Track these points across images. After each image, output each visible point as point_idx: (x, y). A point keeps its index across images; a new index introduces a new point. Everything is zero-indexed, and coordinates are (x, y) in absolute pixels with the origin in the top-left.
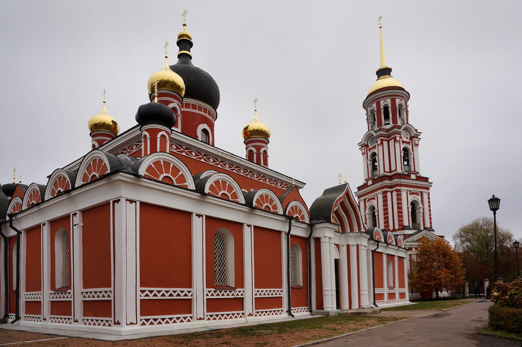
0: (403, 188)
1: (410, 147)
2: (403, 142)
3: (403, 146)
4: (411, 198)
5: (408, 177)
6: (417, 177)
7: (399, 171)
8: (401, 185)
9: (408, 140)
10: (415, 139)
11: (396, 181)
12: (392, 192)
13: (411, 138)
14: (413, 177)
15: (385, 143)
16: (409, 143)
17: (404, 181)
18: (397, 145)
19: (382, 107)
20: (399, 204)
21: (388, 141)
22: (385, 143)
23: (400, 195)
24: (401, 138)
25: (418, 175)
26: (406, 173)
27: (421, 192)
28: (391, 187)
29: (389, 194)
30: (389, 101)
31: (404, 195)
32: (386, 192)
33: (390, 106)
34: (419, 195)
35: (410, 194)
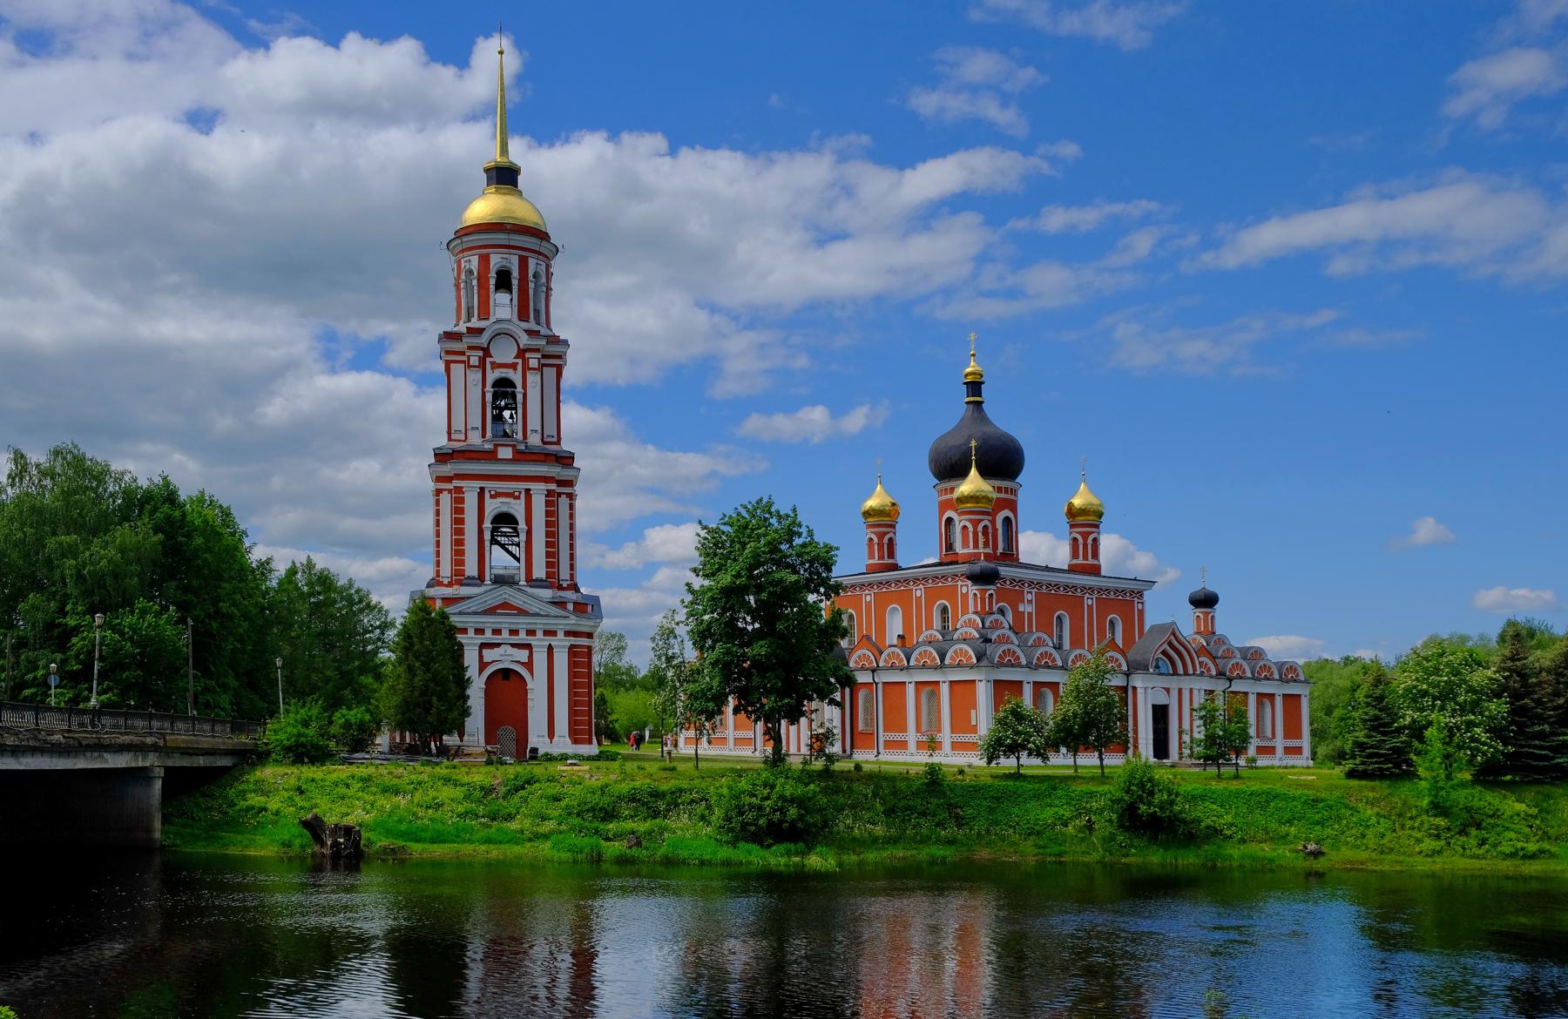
1: (516, 377)
2: (495, 366)
3: (492, 376)
4: (493, 507)
5: (491, 456)
6: (516, 452)
7: (475, 439)
9: (510, 359)
10: (528, 355)
12: (450, 491)
13: (521, 353)
14: (505, 453)
15: (458, 370)
16: (513, 366)
20: (458, 521)
22: (458, 370)
23: (462, 500)
24: (487, 352)
26: (488, 446)
27: (528, 491)
34: (518, 498)
35: (492, 497)
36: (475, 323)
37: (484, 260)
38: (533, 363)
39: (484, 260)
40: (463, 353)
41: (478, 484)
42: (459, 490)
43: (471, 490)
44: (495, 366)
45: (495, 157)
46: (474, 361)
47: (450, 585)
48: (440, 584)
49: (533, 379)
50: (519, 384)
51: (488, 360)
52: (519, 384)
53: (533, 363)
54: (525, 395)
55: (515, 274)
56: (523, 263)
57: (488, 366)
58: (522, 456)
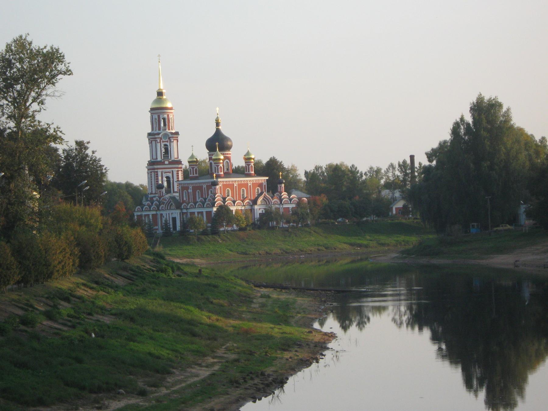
0: (159, 170)
1: (168, 144)
2: (163, 142)
5: (163, 163)
7: (159, 159)
8: (158, 169)
11: (156, 167)
13: (169, 138)
14: (166, 162)
15: (154, 143)
16: (167, 141)
17: (159, 166)
18: (159, 145)
22: (154, 143)
23: (157, 174)
28: (154, 169)
29: (153, 174)
31: (160, 174)
32: (151, 172)
36: (158, 131)
39: (159, 117)
41: (161, 170)
42: (157, 172)
43: (160, 172)
44: (163, 142)
46: (159, 141)
47: (155, 194)
48: (153, 194)
56: (168, 116)
58: (170, 163)
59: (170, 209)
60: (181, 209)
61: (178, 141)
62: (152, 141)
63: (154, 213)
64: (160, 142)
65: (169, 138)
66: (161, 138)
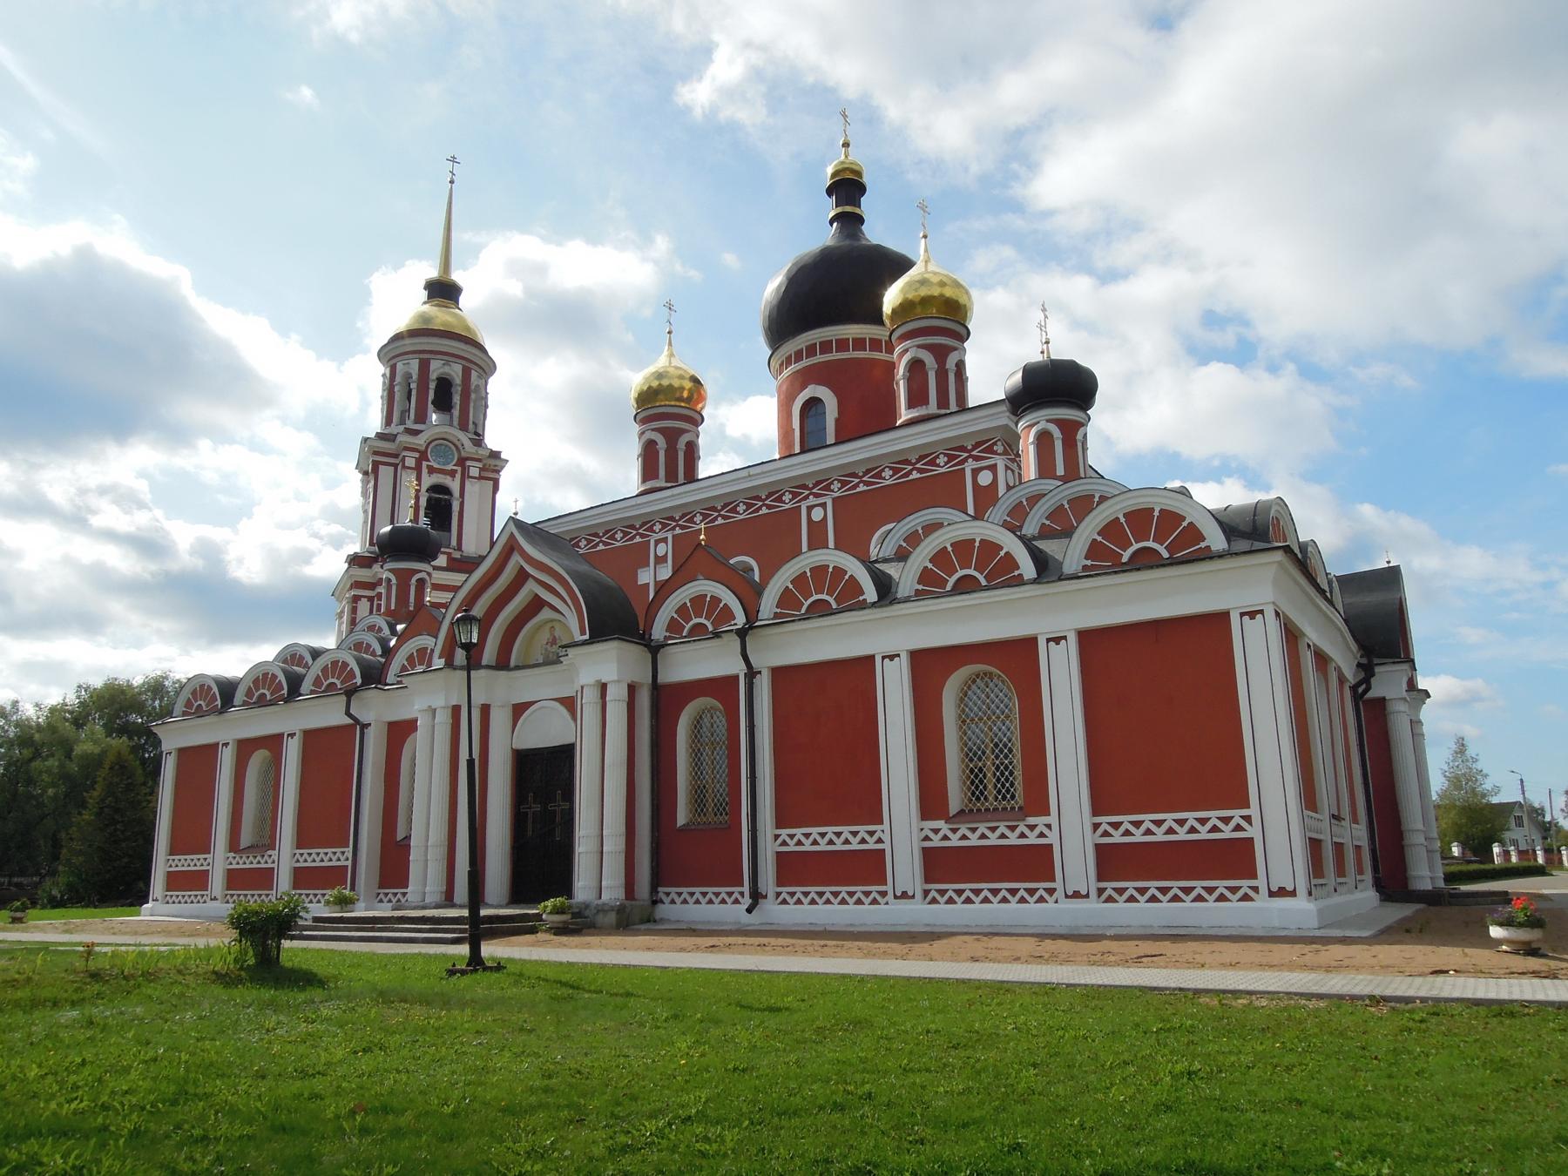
1: (455, 486)
3: (428, 481)
6: (451, 559)
9: (450, 467)
10: (468, 463)
12: (371, 599)
13: (462, 462)
16: (452, 474)
19: (398, 379)
21: (396, 466)
22: (386, 473)
25: (457, 555)
30: (414, 366)
32: (356, 599)
33: (415, 377)
36: (410, 424)
37: (424, 366)
38: (474, 472)
40: (396, 456)
44: (431, 470)
45: (434, 273)
46: (410, 462)
49: (472, 488)
50: (456, 493)
51: (425, 464)
52: (456, 493)
53: (474, 472)
54: (462, 504)
55: (458, 380)
57: (425, 471)
59: (502, 664)
60: (654, 649)
61: (496, 488)
62: (376, 465)
63: (330, 714)
64: (418, 468)
65: (462, 462)
66: (423, 456)
